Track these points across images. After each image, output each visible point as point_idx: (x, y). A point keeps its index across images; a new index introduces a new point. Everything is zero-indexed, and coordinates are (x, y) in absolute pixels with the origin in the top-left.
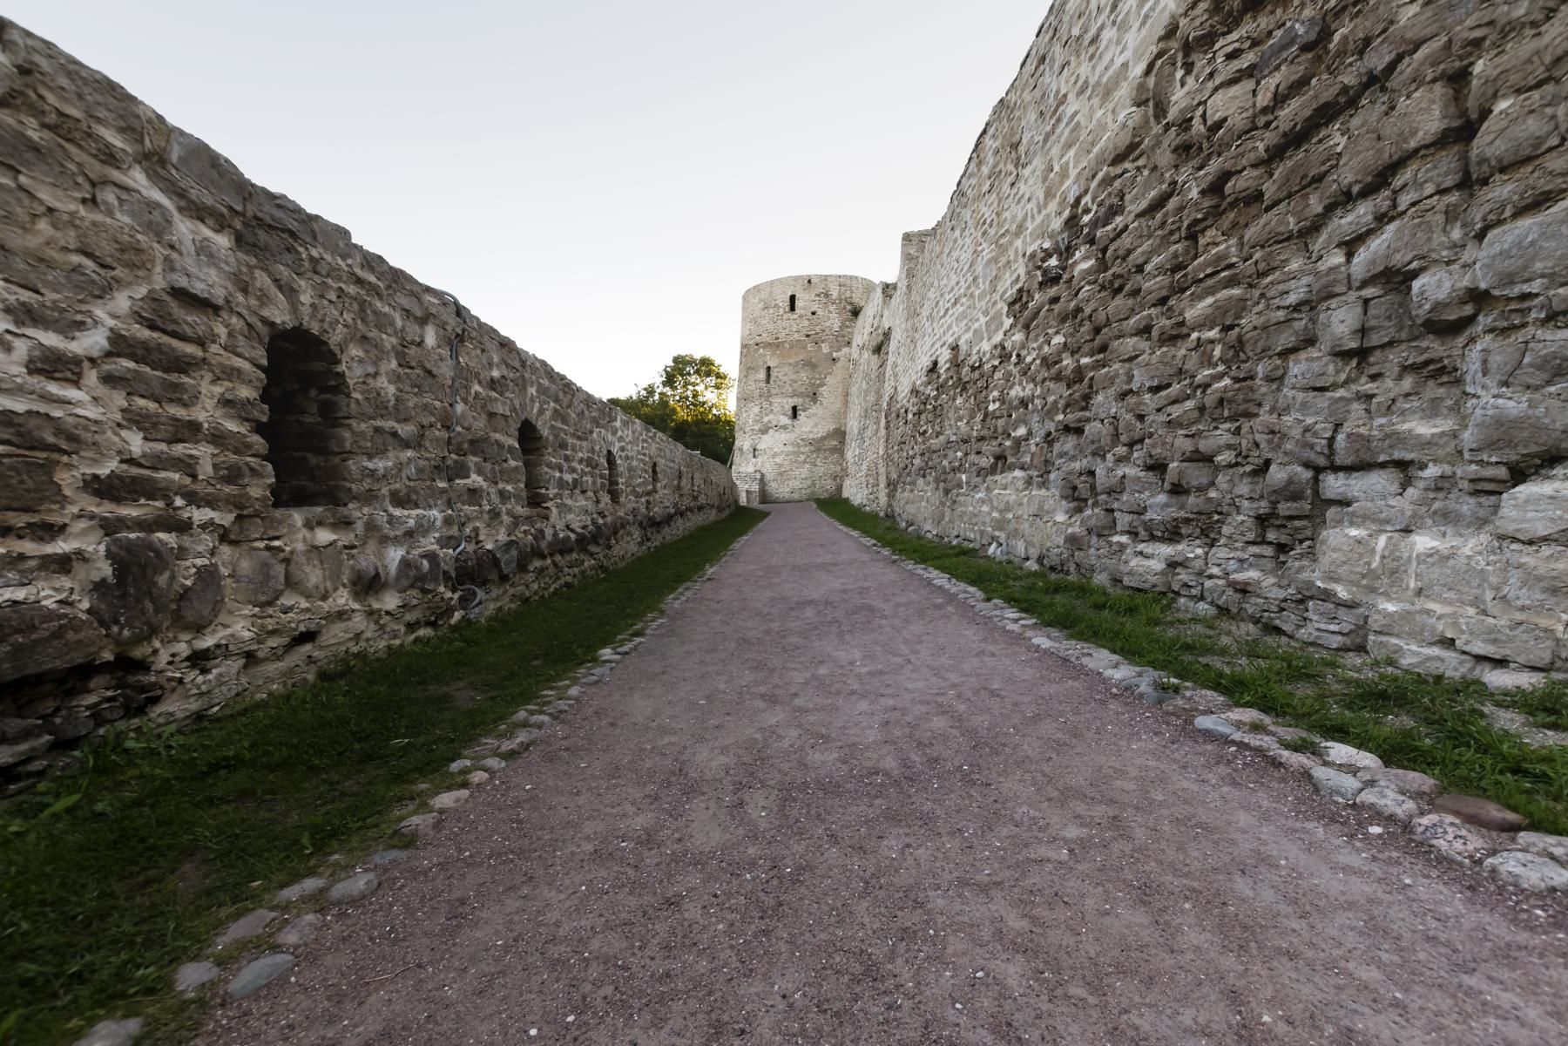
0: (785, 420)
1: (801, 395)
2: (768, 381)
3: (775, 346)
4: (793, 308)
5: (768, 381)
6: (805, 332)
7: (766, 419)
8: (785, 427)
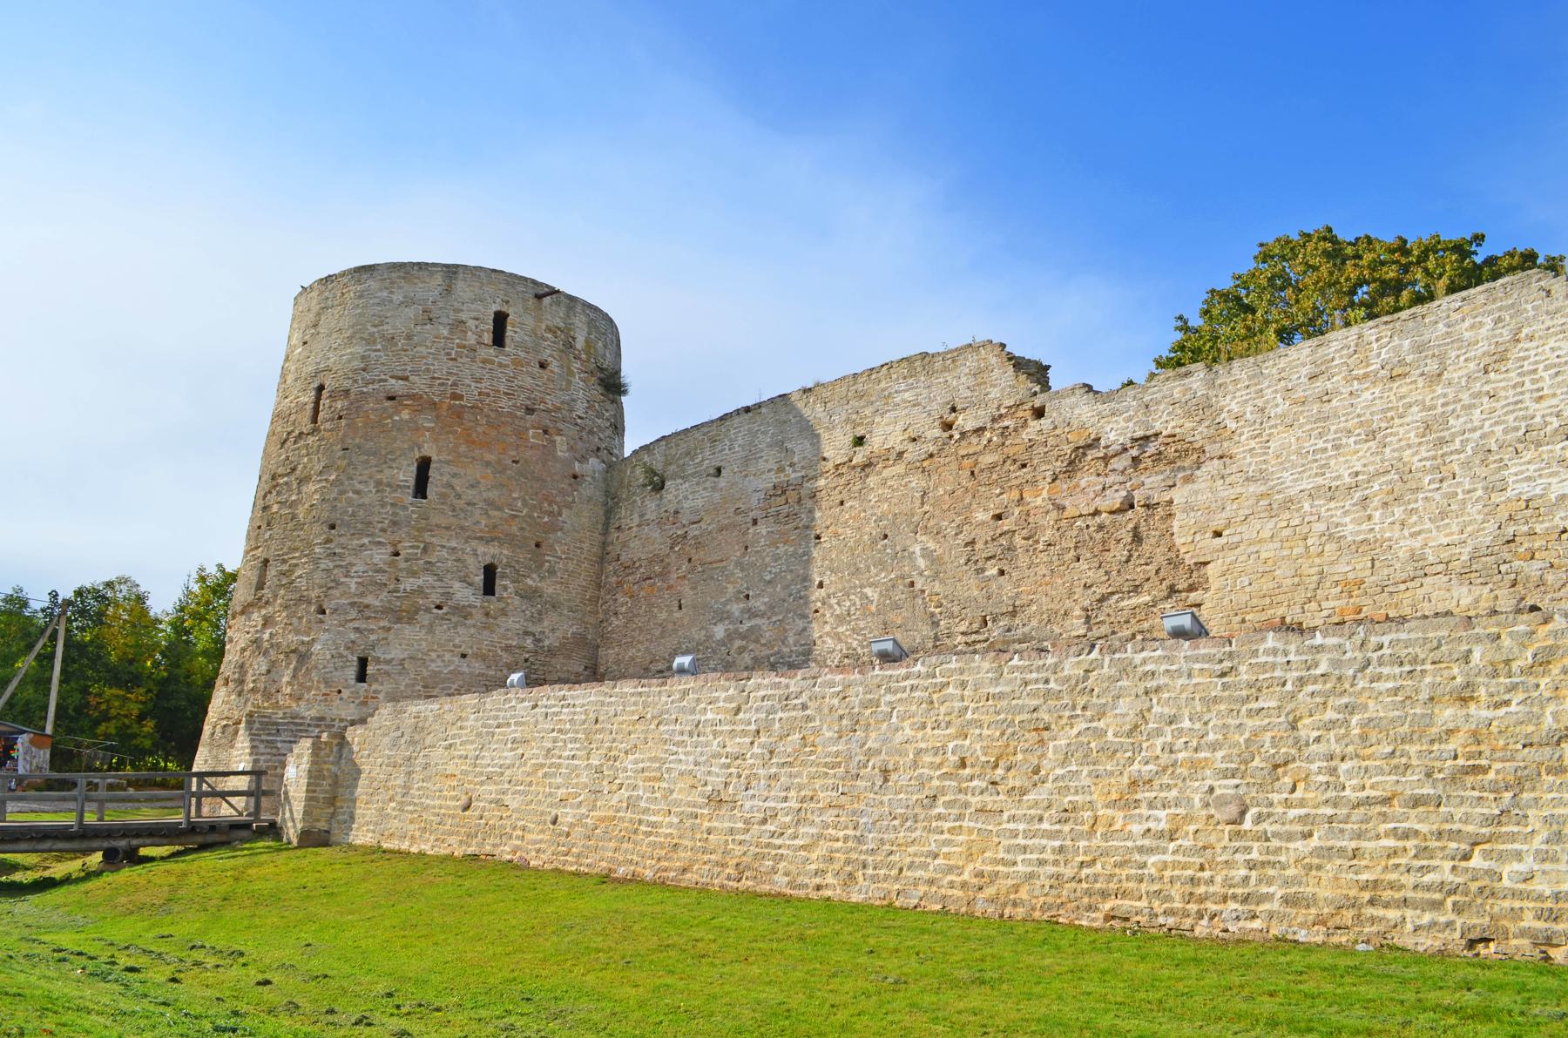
0: (465, 594)
1: (510, 540)
3: (453, 410)
4: (499, 340)
6: (521, 399)
7: (408, 584)
8: (463, 612)
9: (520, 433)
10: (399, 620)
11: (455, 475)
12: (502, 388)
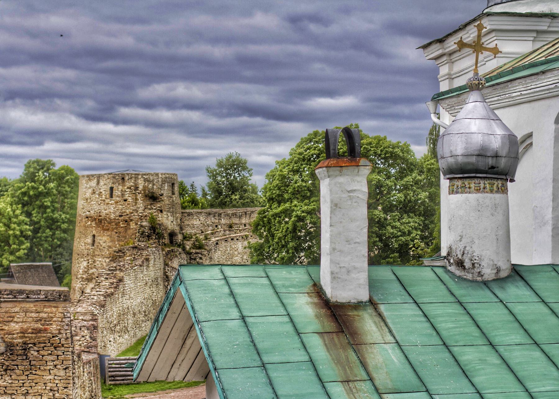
2: (93, 245)
4: (111, 196)
5: (93, 245)
6: (118, 214)
7: (91, 271)
9: (117, 224)
10: (89, 282)
11: (100, 240)
12: (112, 211)
